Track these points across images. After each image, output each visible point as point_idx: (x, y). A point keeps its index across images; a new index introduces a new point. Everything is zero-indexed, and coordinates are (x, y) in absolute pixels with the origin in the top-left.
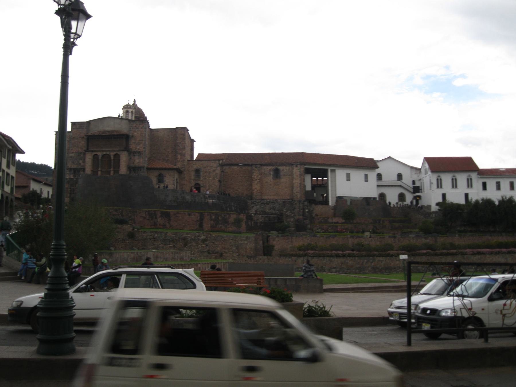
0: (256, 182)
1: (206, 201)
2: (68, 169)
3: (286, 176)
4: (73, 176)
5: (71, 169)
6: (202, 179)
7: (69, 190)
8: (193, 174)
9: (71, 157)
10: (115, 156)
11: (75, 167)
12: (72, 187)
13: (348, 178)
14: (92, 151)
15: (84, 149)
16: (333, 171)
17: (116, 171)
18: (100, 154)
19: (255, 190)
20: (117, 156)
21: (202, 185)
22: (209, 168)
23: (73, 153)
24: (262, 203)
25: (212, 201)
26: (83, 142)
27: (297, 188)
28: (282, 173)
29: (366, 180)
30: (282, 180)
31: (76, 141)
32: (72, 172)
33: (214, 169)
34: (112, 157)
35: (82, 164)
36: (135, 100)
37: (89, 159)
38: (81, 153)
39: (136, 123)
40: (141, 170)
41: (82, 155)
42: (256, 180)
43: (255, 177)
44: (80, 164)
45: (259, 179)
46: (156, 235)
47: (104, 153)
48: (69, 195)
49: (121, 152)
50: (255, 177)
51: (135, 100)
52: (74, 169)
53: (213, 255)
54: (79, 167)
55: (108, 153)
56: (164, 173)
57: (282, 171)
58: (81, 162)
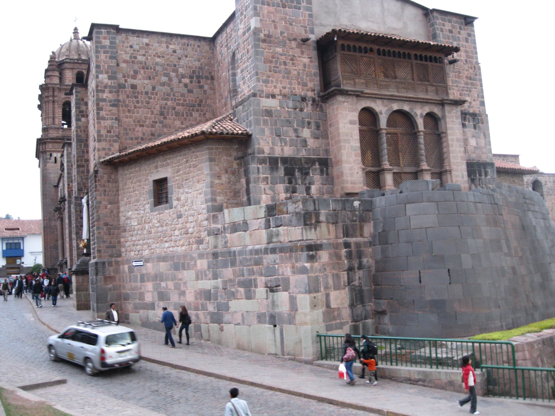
2: (262, 161)
3: (551, 195)
4: (287, 191)
5: (273, 162)
7: (344, 251)
9: (269, 113)
10: (430, 116)
11: (288, 152)
12: (352, 240)
14: (359, 95)
15: (310, 85)
23: (273, 96)
26: (306, 60)
31: (279, 50)
32: (281, 172)
34: (420, 122)
35: (311, 143)
37: (352, 123)
38: (304, 99)
39: (450, 21)
40: (486, 175)
41: (308, 108)
44: (305, 141)
47: (395, 106)
48: (344, 276)
49: (447, 108)
52: (285, 160)
54: (303, 154)
55: (406, 107)
57: (545, 184)
58: (306, 133)
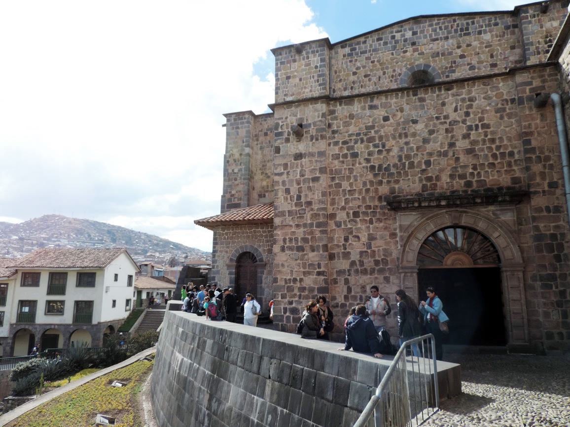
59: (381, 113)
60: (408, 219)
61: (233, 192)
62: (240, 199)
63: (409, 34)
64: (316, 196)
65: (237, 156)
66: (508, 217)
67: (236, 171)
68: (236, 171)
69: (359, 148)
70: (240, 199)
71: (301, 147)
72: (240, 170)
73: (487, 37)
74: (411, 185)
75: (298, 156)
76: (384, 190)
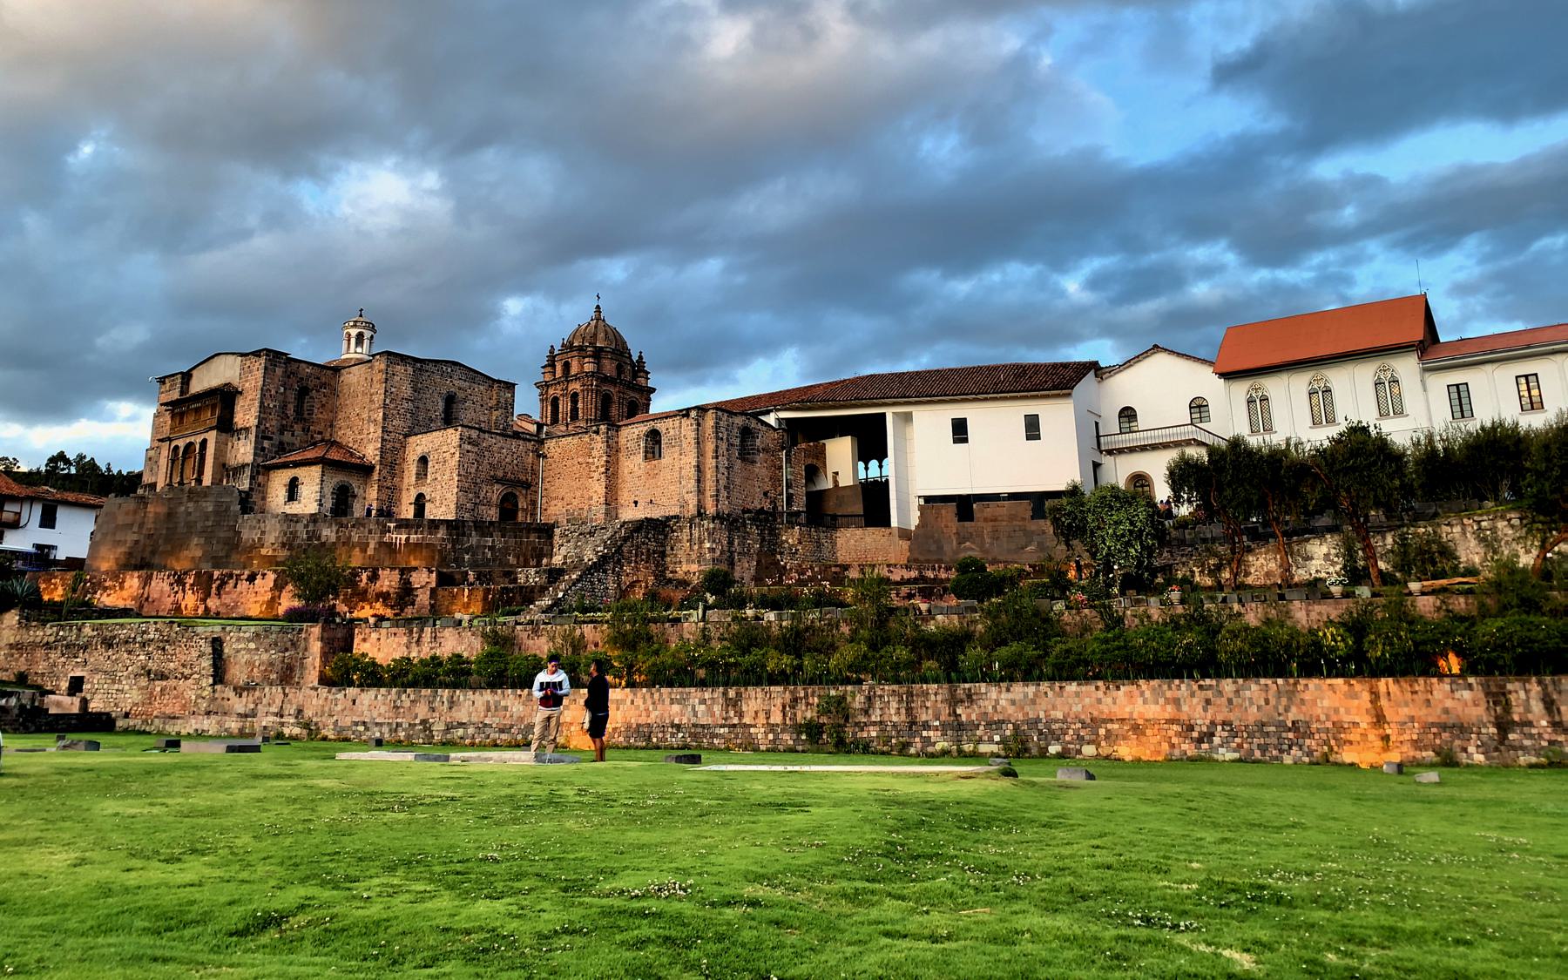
0: (596, 475)
1: (386, 539)
6: (428, 481)
8: (411, 469)
13: (960, 430)
16: (908, 418)
17: (199, 481)
18: (181, 443)
19: (595, 498)
20: (204, 443)
21: (428, 498)
22: (444, 449)
24: (580, 534)
25: (407, 539)
27: (690, 478)
28: (664, 440)
29: (1033, 428)
30: (663, 461)
33: (453, 450)
36: (598, 307)
42: (597, 467)
43: (596, 460)
45: (602, 466)
46: (61, 633)
50: (596, 460)
51: (598, 307)
53: (157, 683)
56: (300, 472)
59: (494, 441)
60: (496, 486)
61: (268, 425)
62: (273, 433)
63: (449, 370)
64: (473, 471)
65: (273, 392)
66: (524, 492)
67: (271, 406)
68: (271, 406)
69: (486, 453)
70: (273, 433)
71: (469, 447)
72: (275, 406)
73: (482, 388)
74: (500, 474)
75: (468, 451)
76: (492, 473)
